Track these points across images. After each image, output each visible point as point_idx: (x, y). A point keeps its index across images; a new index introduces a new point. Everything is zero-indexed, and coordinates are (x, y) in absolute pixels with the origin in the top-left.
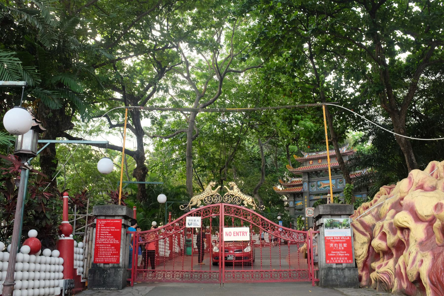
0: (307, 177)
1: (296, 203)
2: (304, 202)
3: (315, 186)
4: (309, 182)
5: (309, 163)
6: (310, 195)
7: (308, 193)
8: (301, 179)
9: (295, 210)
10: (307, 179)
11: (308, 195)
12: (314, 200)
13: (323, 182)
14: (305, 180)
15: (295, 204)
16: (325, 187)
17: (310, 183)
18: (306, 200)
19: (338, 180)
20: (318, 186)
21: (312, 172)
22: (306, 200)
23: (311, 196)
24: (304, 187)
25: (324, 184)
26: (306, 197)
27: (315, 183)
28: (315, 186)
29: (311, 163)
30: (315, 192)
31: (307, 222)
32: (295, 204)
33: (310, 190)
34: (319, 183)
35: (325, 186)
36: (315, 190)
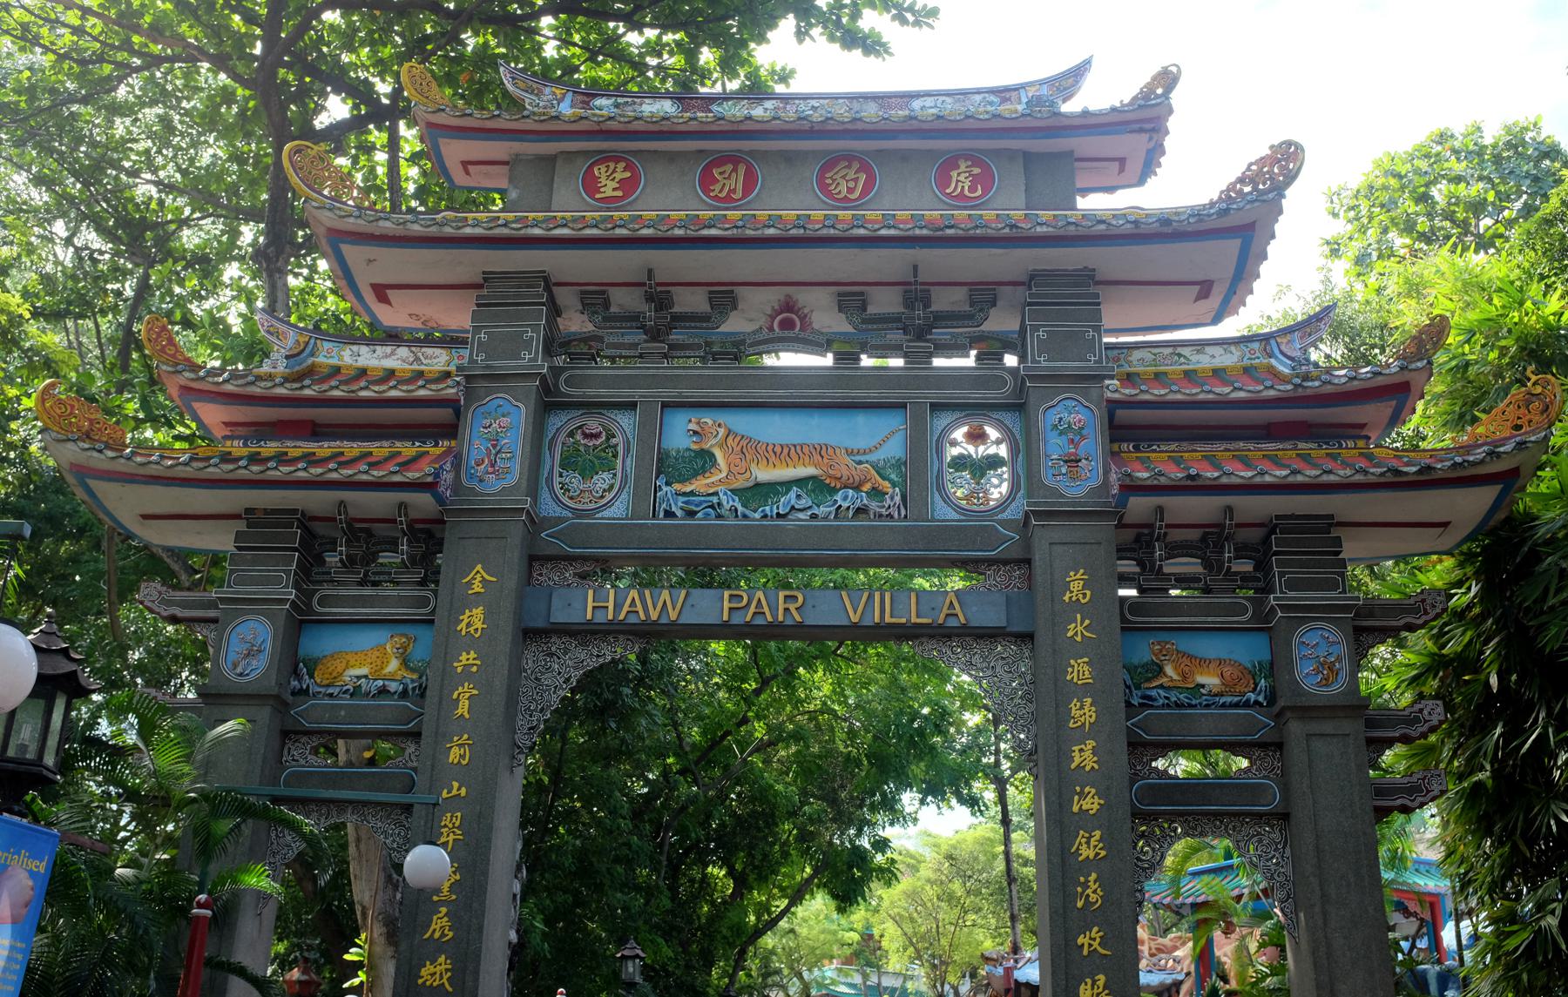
0: (534, 335)
1: (320, 643)
2: (449, 645)
3: (626, 464)
4: (549, 401)
5: (591, 185)
6: (535, 559)
7: (516, 533)
8: (438, 359)
9: (288, 734)
10: (532, 358)
11: (514, 555)
12: (586, 633)
13: (743, 422)
14: (505, 365)
15: (293, 662)
16: (762, 492)
17: (557, 421)
18: (474, 620)
19: (944, 420)
20: (670, 467)
21: (594, 298)
22: (474, 620)
23: (548, 576)
24: (475, 443)
25: (749, 449)
26: (478, 579)
27: (626, 422)
28: (626, 464)
29: (609, 188)
30: (616, 530)
31: (440, 925)
32: (293, 662)
33: (549, 508)
34: (679, 433)
35: (764, 474)
36: (618, 510)
